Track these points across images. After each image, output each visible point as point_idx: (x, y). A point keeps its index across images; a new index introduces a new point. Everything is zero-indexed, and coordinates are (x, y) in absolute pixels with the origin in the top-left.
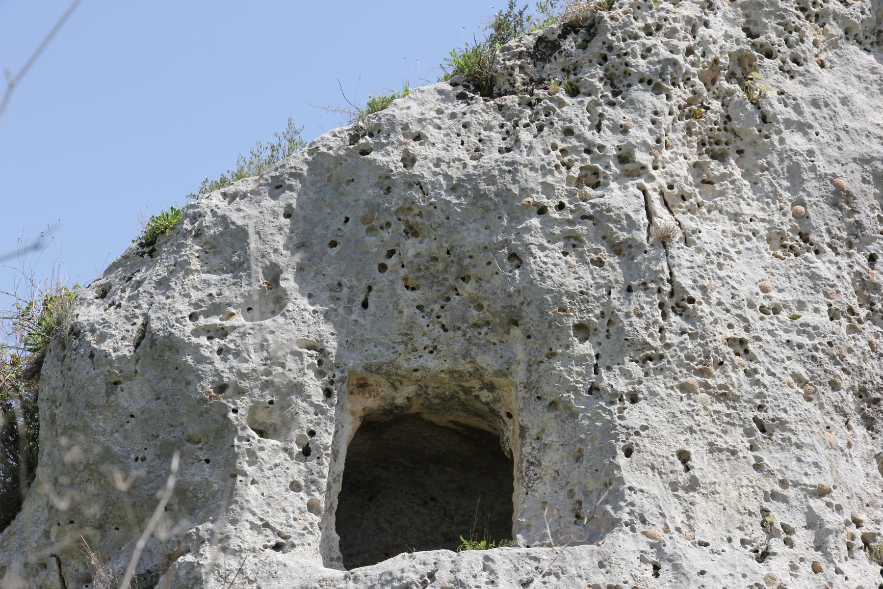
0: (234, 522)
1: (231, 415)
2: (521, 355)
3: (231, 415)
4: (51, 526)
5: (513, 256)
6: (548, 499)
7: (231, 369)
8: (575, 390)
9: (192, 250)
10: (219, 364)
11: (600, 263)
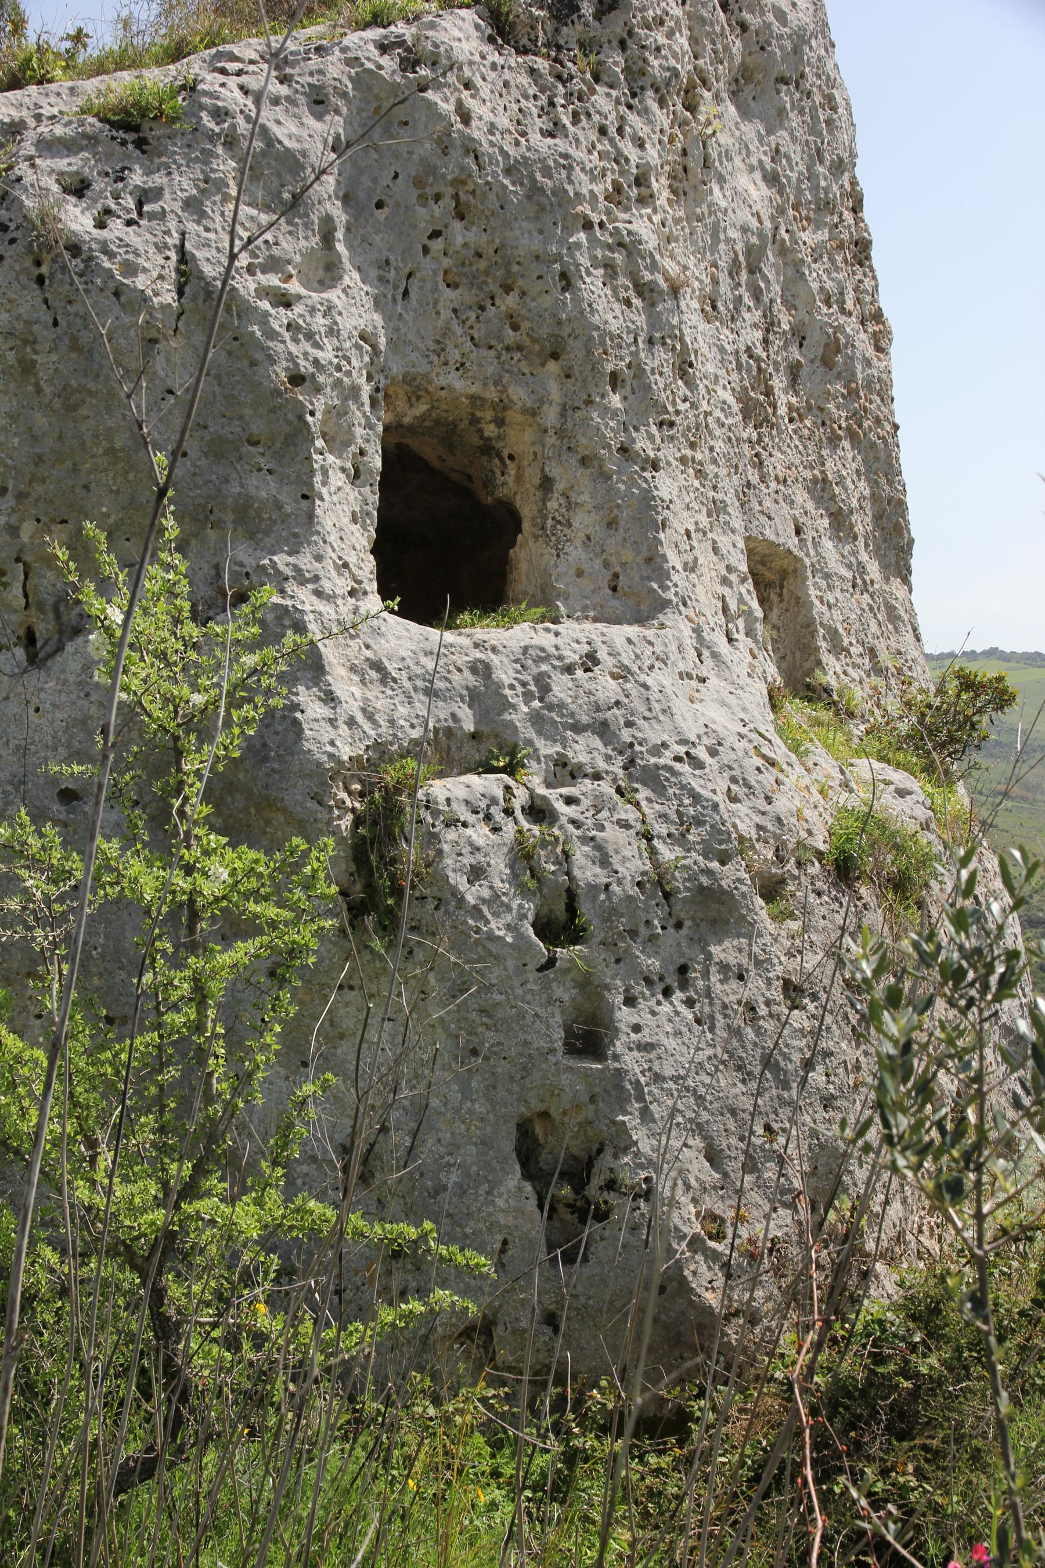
0: (319, 558)
1: (309, 419)
2: (555, 395)
3: (309, 419)
4: (22, 520)
5: (563, 275)
6: (585, 566)
7: (306, 354)
8: (609, 446)
9: (226, 166)
10: (292, 347)
11: (628, 303)
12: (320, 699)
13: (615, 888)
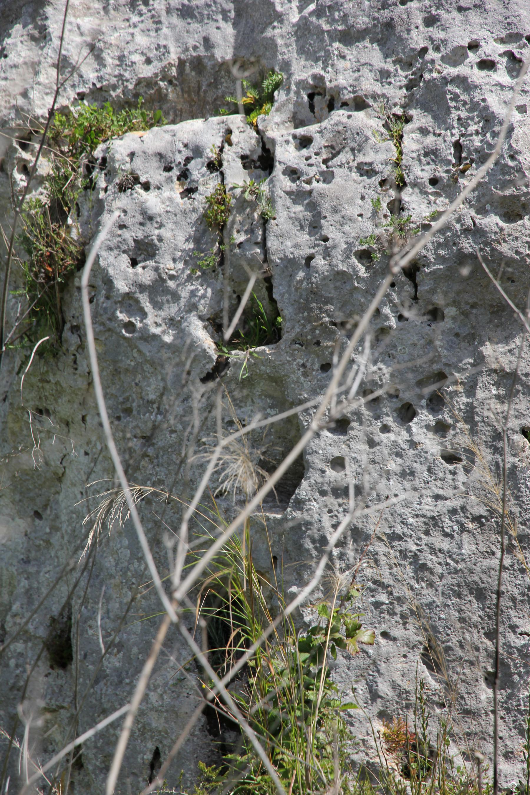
12: (33, 38)
13: (319, 262)
